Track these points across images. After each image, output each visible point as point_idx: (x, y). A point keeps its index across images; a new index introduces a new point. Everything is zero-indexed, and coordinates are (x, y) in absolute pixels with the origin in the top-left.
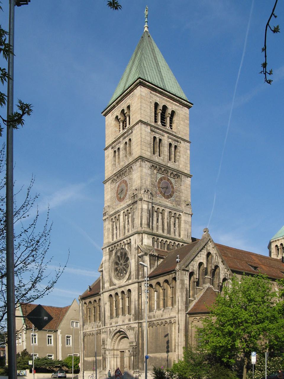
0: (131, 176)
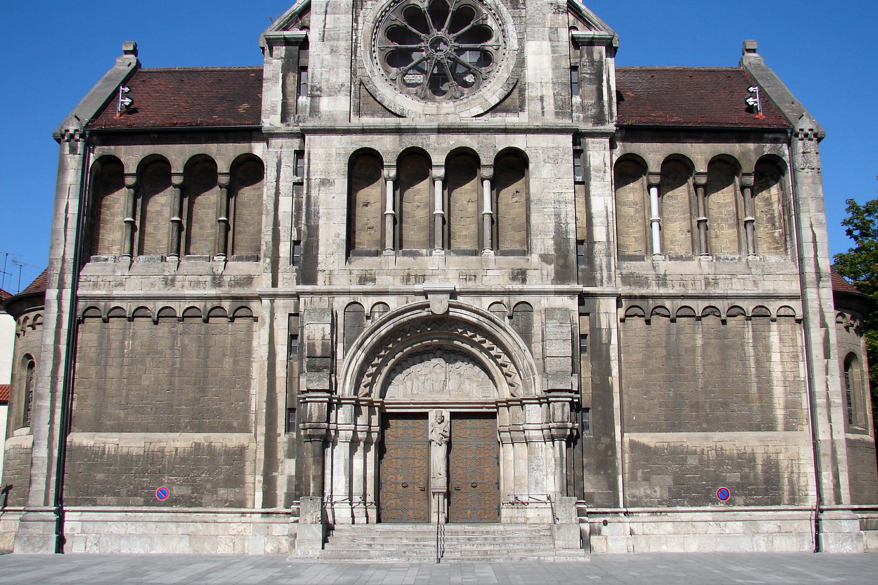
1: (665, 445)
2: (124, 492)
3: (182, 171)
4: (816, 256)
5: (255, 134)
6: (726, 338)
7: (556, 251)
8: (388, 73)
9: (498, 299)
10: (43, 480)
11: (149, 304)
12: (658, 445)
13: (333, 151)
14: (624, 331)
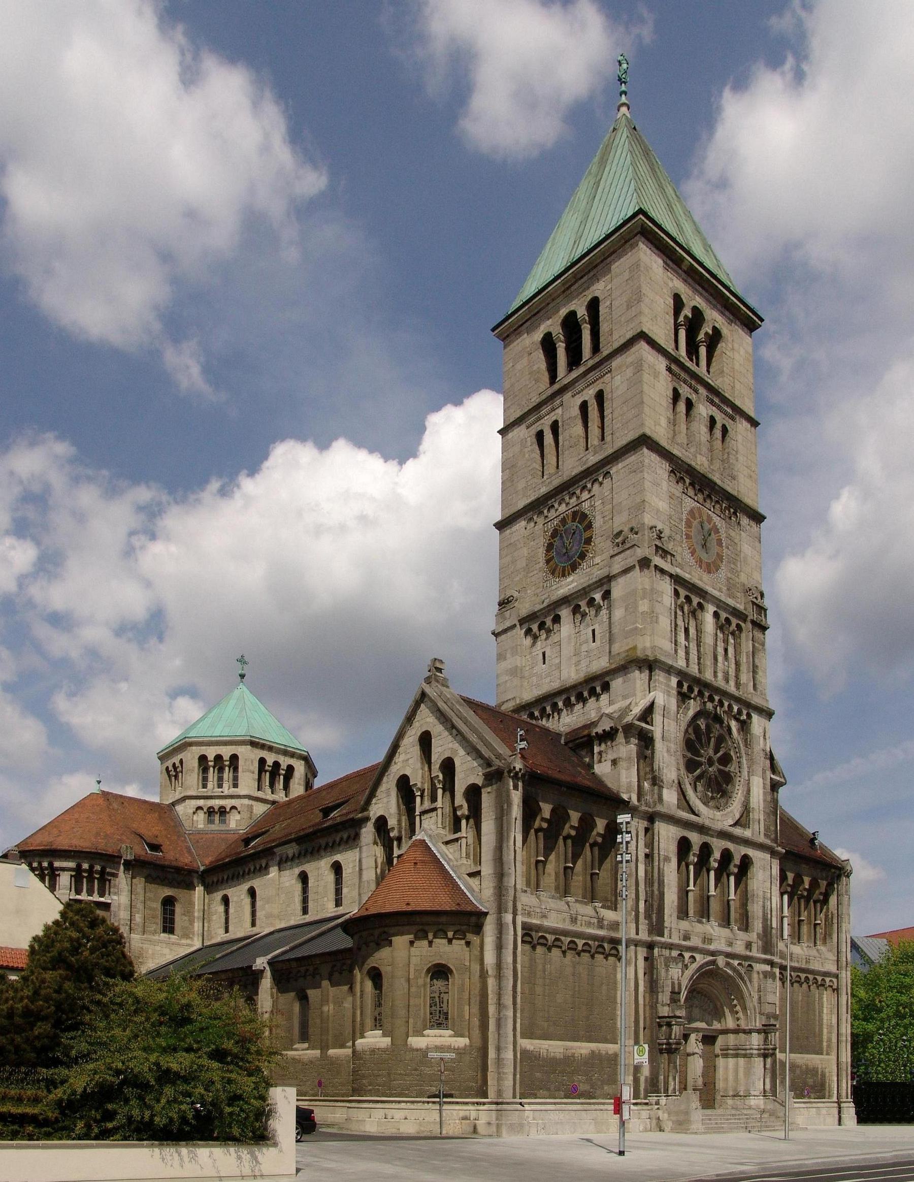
2: (552, 1088)
10: (511, 1077)
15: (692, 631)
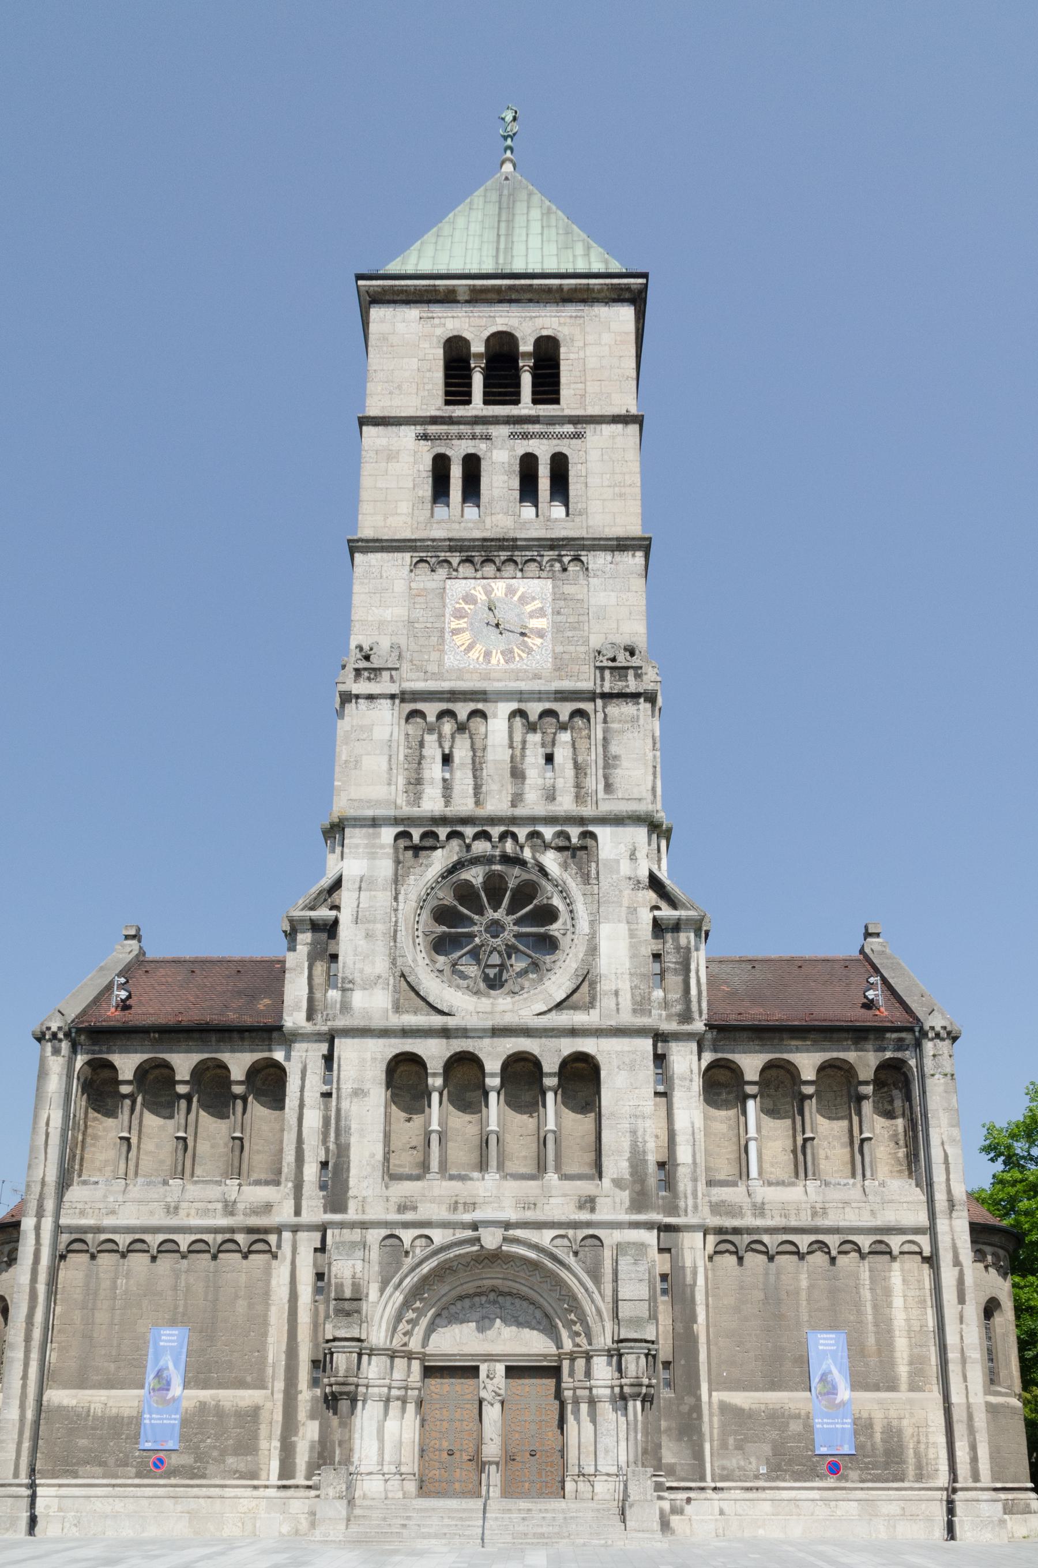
0: (568, 589)
1: (763, 1407)
2: (111, 1461)
3: (187, 1078)
4: (948, 1180)
5: (275, 1035)
6: (835, 1278)
7: (632, 1175)
8: (434, 962)
9: (562, 1232)
11: (147, 1237)
12: (753, 1406)
13: (368, 1056)
14: (713, 1270)
15: (462, 753)
